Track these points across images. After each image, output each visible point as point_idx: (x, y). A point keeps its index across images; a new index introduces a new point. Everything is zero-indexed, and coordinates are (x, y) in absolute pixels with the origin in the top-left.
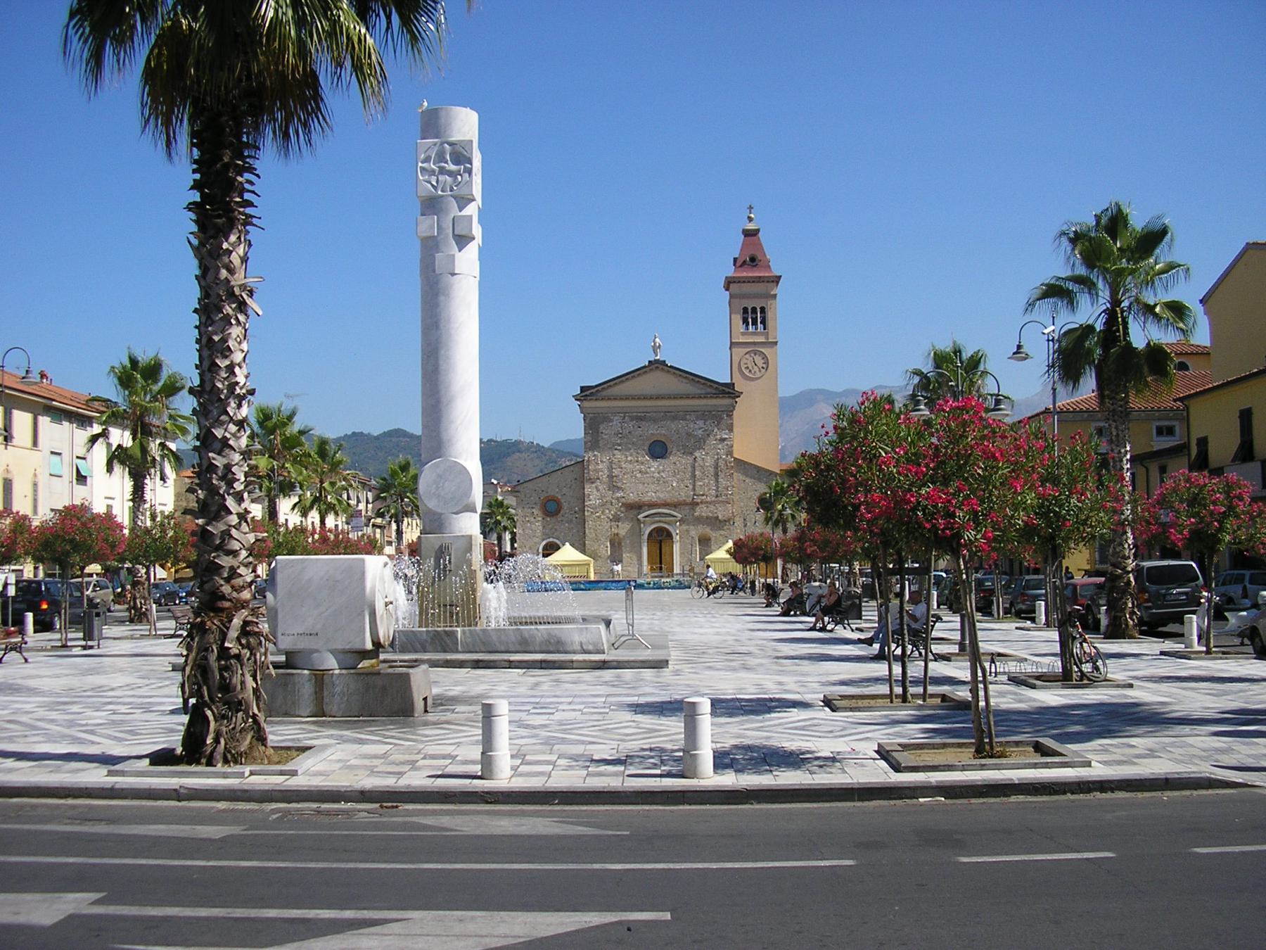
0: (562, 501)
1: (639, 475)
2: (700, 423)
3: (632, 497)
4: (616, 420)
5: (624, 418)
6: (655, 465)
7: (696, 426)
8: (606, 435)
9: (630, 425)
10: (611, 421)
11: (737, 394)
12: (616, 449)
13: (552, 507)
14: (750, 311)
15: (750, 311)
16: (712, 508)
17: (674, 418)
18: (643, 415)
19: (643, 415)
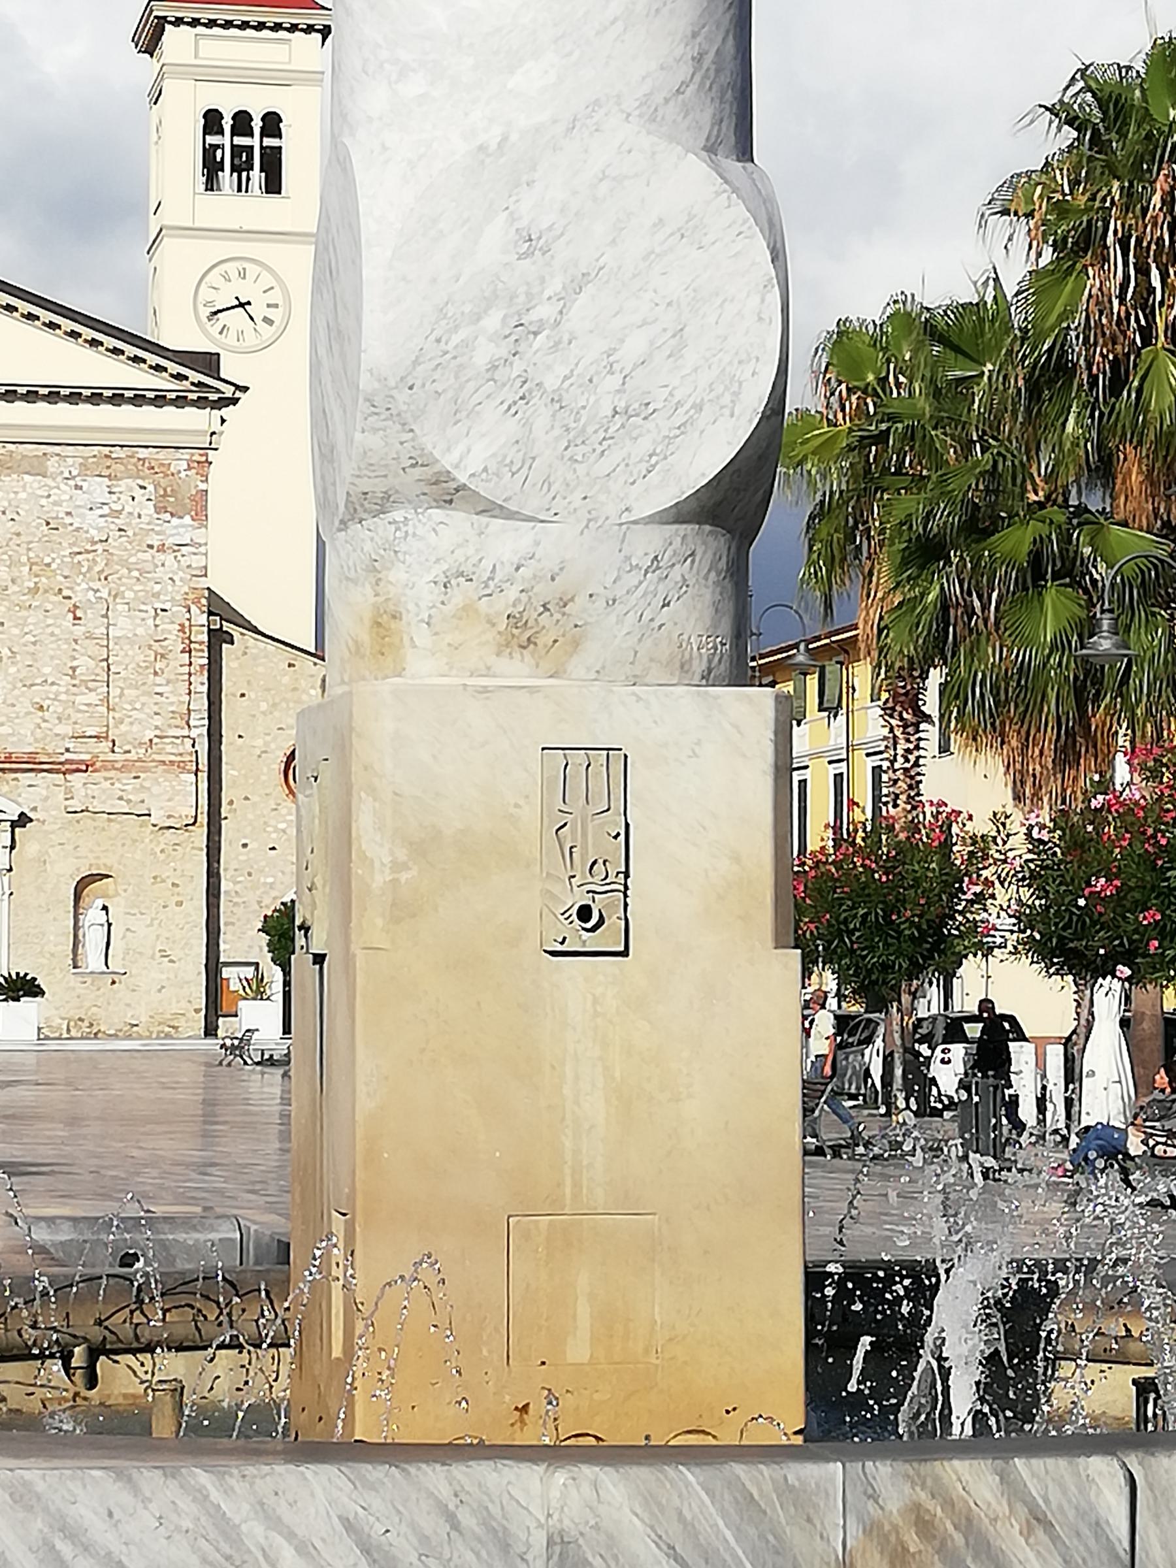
2: (97, 488)
7: (81, 498)
11: (228, 391)
14: (257, 125)
15: (257, 125)
16: (126, 783)
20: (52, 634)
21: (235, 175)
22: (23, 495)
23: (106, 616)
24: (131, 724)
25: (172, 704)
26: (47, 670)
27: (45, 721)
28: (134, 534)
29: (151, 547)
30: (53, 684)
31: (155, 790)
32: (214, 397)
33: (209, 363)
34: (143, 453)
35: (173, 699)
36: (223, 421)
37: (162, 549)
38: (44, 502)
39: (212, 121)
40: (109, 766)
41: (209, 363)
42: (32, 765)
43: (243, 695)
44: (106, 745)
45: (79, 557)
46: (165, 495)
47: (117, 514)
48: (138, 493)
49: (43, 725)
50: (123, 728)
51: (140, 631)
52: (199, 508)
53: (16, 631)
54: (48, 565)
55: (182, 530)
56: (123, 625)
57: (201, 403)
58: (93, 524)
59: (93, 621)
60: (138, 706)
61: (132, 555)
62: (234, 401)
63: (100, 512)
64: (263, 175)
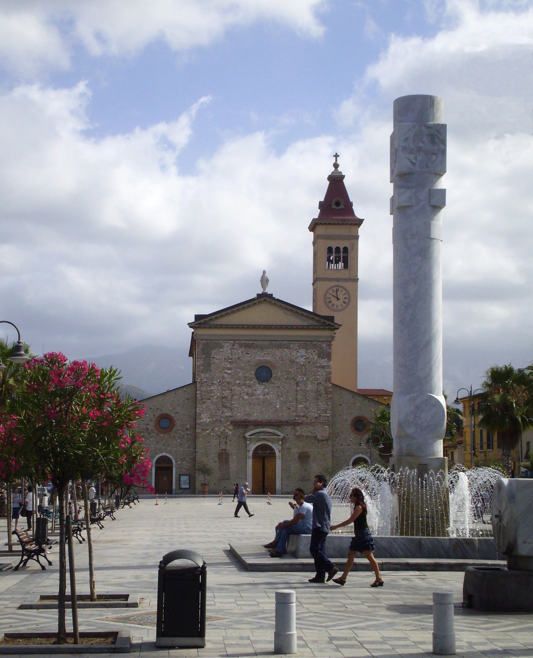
0: (175, 419)
1: (246, 397)
3: (240, 416)
4: (227, 347)
5: (234, 345)
6: (260, 389)
7: (299, 354)
8: (217, 359)
9: (239, 351)
10: (222, 347)
12: (226, 373)
13: (165, 423)
16: (311, 428)
17: (279, 347)
18: (251, 342)
19: (251, 342)
20: (292, 389)
21: (335, 265)
22: (284, 354)
23: (305, 385)
24: (312, 413)
25: (322, 407)
26: (290, 399)
27: (290, 412)
28: (313, 363)
29: (317, 367)
30: (292, 402)
31: (319, 430)
32: (333, 328)
33: (331, 319)
34: (314, 343)
35: (322, 406)
36: (335, 333)
37: (319, 367)
38: (289, 355)
39: (330, 250)
40: (307, 424)
41: (331, 319)
42: (287, 423)
43: (340, 405)
44: (305, 418)
45: (299, 370)
46: (320, 353)
47: (307, 358)
48: (313, 353)
49: (290, 413)
50: (310, 414)
51: (314, 388)
52: (328, 356)
53: (282, 389)
54: (290, 372)
55: (325, 362)
56: (309, 387)
57: (329, 329)
58: (302, 360)
59: (302, 386)
60: (314, 408)
61: (312, 369)
62: (338, 329)
63: (304, 358)
64: (343, 264)
